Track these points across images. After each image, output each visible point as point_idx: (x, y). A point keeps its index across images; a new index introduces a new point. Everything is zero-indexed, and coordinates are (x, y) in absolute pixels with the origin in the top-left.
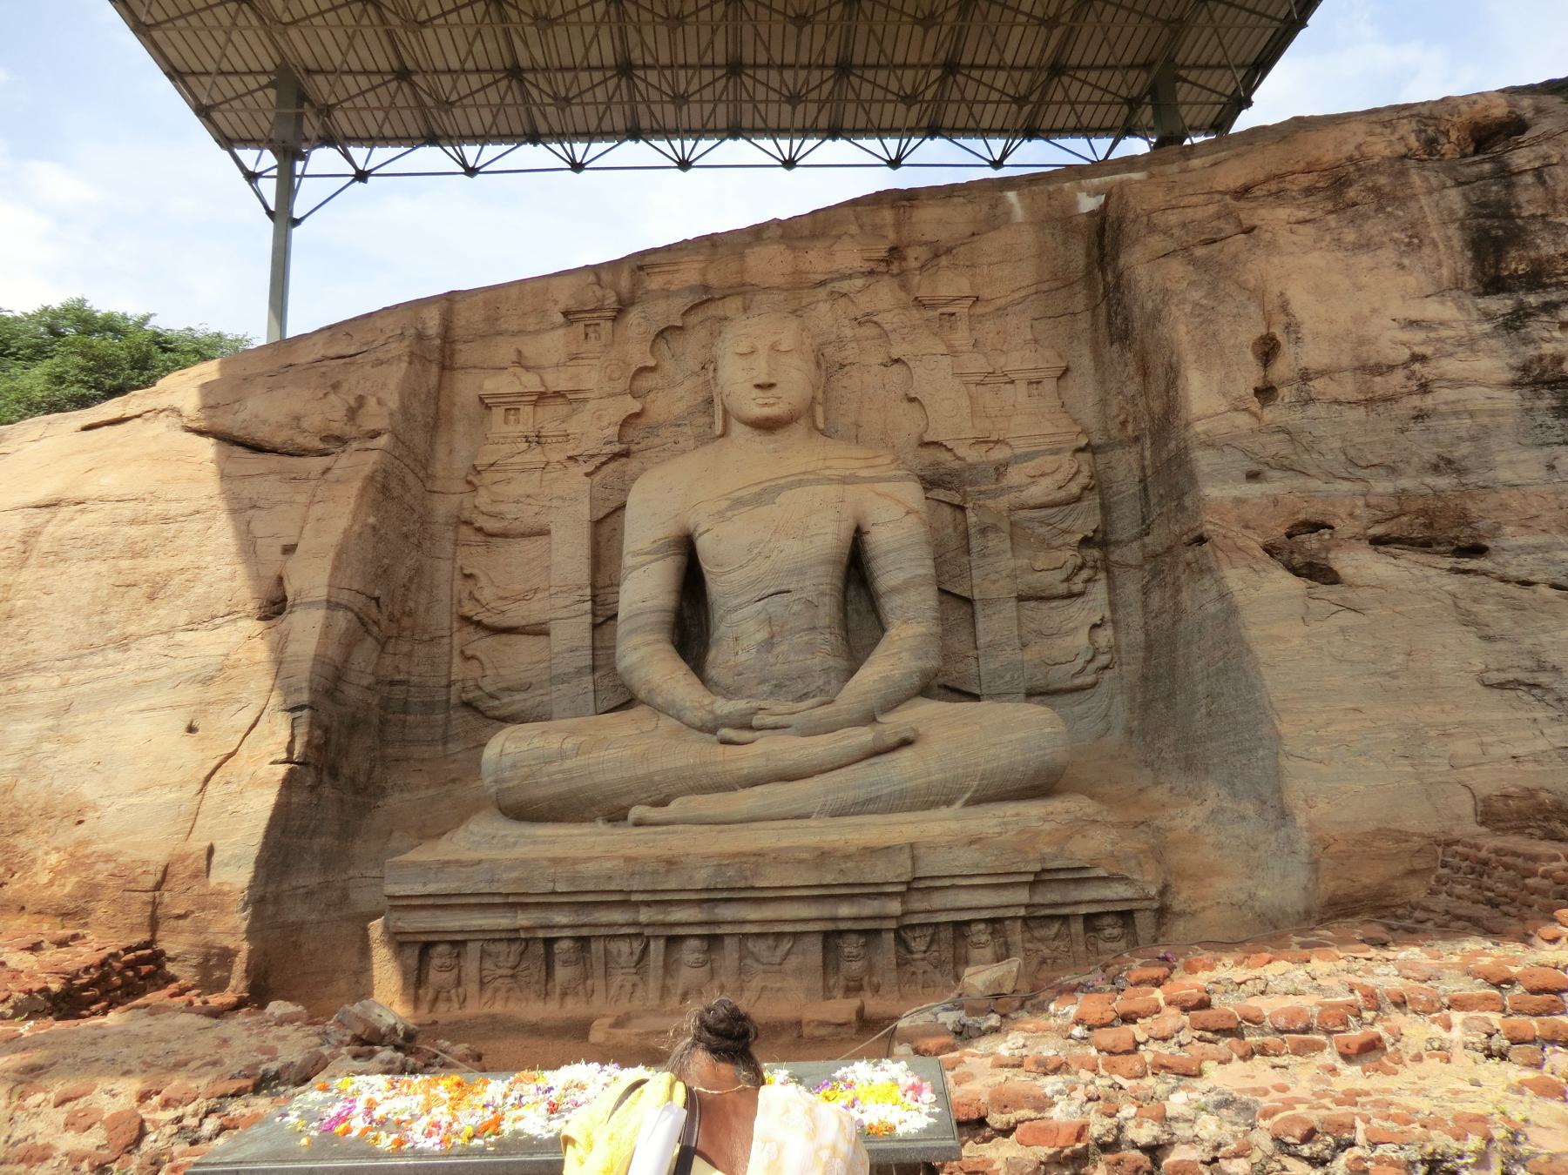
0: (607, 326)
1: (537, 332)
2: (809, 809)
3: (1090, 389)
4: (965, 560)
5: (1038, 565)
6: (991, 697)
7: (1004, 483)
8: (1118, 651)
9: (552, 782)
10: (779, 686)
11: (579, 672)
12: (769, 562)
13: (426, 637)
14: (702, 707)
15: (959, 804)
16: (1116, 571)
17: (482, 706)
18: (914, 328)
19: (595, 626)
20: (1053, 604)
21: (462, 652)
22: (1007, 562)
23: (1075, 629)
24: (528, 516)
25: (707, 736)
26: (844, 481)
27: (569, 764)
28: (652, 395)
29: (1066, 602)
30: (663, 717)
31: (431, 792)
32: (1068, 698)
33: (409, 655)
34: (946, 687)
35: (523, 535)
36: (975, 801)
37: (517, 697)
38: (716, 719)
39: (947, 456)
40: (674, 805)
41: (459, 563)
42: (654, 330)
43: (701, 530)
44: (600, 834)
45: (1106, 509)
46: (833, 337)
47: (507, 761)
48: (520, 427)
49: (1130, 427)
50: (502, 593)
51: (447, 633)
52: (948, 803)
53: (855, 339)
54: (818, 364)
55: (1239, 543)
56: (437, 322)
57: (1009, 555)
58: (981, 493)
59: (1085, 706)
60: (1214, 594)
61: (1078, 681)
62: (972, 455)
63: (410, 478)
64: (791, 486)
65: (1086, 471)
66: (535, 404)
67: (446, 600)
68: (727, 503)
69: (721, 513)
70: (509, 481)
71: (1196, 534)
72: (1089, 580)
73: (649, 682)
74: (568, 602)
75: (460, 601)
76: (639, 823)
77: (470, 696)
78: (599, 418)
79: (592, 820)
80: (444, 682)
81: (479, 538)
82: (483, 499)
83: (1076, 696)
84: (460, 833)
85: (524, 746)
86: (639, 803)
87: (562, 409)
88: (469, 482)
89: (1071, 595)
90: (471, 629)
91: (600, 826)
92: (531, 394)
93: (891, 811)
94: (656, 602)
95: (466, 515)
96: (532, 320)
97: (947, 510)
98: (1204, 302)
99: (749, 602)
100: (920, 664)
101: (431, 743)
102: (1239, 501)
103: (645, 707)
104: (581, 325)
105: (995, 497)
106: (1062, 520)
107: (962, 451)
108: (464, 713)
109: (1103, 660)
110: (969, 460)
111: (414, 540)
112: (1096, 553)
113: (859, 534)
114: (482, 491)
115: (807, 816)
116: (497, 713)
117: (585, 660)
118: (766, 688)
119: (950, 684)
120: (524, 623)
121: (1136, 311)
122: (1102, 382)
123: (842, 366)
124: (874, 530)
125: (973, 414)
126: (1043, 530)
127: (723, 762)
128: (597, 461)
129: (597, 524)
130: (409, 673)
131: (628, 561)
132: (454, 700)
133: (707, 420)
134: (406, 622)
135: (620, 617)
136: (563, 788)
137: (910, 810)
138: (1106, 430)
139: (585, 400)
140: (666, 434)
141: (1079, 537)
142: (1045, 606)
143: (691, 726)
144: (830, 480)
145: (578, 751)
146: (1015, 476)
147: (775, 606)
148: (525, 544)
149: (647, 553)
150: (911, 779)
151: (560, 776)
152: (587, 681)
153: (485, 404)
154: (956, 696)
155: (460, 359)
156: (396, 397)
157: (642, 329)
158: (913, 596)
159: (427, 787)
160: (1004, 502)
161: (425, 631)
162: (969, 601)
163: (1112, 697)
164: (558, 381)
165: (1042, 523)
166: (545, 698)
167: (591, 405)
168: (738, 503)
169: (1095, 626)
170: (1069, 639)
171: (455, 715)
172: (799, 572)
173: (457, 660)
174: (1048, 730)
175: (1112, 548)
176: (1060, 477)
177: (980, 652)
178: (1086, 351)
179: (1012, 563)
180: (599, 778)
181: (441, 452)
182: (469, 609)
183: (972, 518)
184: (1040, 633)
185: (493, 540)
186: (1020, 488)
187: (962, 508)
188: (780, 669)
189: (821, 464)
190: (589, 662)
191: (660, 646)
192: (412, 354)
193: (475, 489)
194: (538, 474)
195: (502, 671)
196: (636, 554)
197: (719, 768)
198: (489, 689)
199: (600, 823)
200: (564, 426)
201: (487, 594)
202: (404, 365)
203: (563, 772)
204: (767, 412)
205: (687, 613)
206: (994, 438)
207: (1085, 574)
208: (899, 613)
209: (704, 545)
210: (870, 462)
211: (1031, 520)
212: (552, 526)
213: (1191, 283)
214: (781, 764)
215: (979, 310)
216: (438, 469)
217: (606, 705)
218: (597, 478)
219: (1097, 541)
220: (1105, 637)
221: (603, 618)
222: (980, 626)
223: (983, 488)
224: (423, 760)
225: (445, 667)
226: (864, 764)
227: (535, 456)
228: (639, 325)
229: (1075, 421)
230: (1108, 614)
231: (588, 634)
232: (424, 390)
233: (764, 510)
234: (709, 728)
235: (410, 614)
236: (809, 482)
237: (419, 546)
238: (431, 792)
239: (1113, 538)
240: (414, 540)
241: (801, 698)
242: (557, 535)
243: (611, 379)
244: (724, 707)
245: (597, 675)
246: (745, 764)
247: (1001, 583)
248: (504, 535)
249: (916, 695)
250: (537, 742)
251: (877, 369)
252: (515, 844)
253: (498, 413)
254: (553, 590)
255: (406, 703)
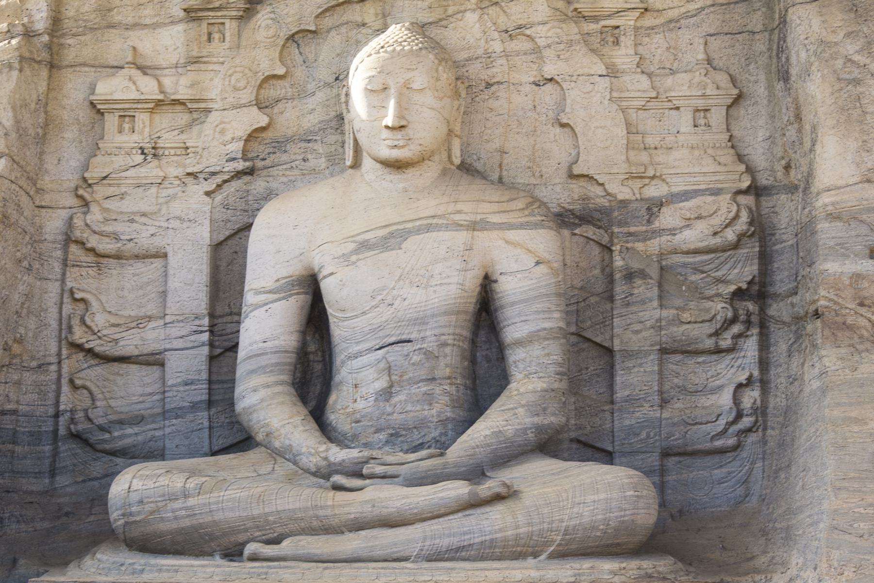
0: (230, 27)
1: (155, 26)
2: (407, 554)
3: (762, 122)
4: (608, 306)
5: (686, 316)
6: (623, 454)
7: (656, 224)
8: (764, 414)
9: (176, 518)
10: (396, 435)
11: (194, 407)
12: (392, 310)
13: (34, 364)
14: (317, 453)
15: (542, 557)
16: (773, 327)
17: (93, 439)
18: (570, 43)
19: (212, 358)
20: (700, 359)
21: (71, 381)
22: (652, 313)
23: (721, 388)
24: (144, 236)
25: (322, 481)
26: (474, 227)
27: (191, 502)
28: (280, 105)
29: (715, 357)
30: (280, 460)
31: (46, 524)
32: (708, 460)
33: (18, 383)
34: (579, 441)
35: (137, 257)
36: (563, 554)
37: (129, 431)
38: (330, 465)
39: (599, 191)
40: (285, 543)
41: (69, 284)
42: (284, 33)
43: (325, 272)
44: (218, 566)
45: (765, 258)
46: (480, 52)
47: (135, 497)
48: (135, 137)
49: (793, 172)
50: (113, 320)
51: (53, 359)
52: (535, 555)
53: (506, 55)
54: (457, 94)
55: (849, 321)
56: (44, 14)
57: (655, 303)
58: (630, 234)
59: (724, 470)
60: (817, 371)
61: (718, 443)
62: (623, 193)
63: (25, 200)
64: (418, 231)
65: (744, 217)
66: (152, 111)
67: (54, 324)
68: (352, 246)
69: (345, 257)
70: (122, 196)
71: (812, 308)
72: (740, 336)
73: (268, 425)
74: (184, 332)
75: (70, 328)
76: (254, 558)
77: (80, 427)
78: (222, 132)
79: (211, 554)
80: (51, 411)
81: (91, 258)
82: (95, 216)
83: (717, 458)
84: (88, 561)
85: (150, 484)
86: (254, 540)
87: (183, 118)
88: (78, 196)
89: (718, 351)
90: (81, 355)
91: (218, 560)
92: (146, 101)
93: (482, 559)
94: (277, 342)
95: (77, 234)
96: (148, 11)
97: (596, 250)
98: (856, 58)
99: (369, 350)
100: (536, 420)
101: (38, 474)
102: (857, 277)
103: (263, 449)
104: (204, 25)
105: (645, 240)
106: (717, 269)
107: (612, 188)
108: (73, 445)
109: (747, 422)
110: (620, 197)
111: (25, 263)
112: (751, 306)
113: (487, 283)
114: (94, 208)
115: (406, 559)
116: (107, 447)
117: (200, 393)
118: (382, 436)
119: (582, 439)
120: (137, 353)
121: (793, 60)
122: (773, 117)
123: (489, 85)
124: (502, 279)
125: (629, 146)
126: (695, 278)
127: (333, 506)
128: (219, 179)
129: (217, 247)
130: (18, 402)
131: (249, 298)
132: (62, 431)
133: (339, 137)
134: (16, 349)
135: (242, 353)
136: (186, 523)
137: (500, 559)
138: (773, 170)
139: (208, 111)
140: (295, 150)
141: (733, 288)
142: (691, 361)
143: (307, 471)
144: (458, 226)
145: (200, 490)
146: (668, 218)
147: (395, 355)
148: (139, 267)
149: (270, 292)
150: (500, 530)
151: (184, 513)
152: (202, 417)
153: (97, 110)
154: (589, 452)
155: (70, 56)
156: (11, 114)
157: (271, 32)
158: (536, 350)
159: (42, 519)
160: (654, 246)
161: (33, 358)
162: (610, 351)
163: (753, 463)
164: (180, 86)
165: (697, 270)
166: (158, 433)
167: (214, 117)
168: (364, 246)
169: (740, 386)
170: (714, 397)
171: (63, 447)
172: (421, 321)
173: (65, 388)
174: (631, 493)
175: (770, 301)
176: (717, 221)
177: (616, 407)
178: (762, 77)
179: (657, 314)
180: (219, 516)
181: (50, 162)
182: (79, 335)
183: (618, 262)
184: (683, 389)
185: (105, 261)
186: (673, 232)
187: (608, 249)
188: (397, 418)
189: (451, 208)
190: (205, 397)
191: (280, 388)
192: (22, 58)
193: (86, 204)
194: (154, 190)
195: (112, 403)
196: (258, 292)
197: (329, 512)
198: (101, 421)
199: (218, 557)
200: (183, 137)
201: (99, 320)
202: (15, 74)
203: (186, 508)
204: (395, 154)
205: (312, 348)
206: (651, 173)
207: (736, 329)
208: (521, 366)
209: (327, 287)
210: (505, 207)
211: (684, 265)
212: (169, 249)
213: (848, 35)
214: (385, 511)
215: (648, 21)
216: (46, 182)
217: (218, 444)
218: (219, 198)
219: (758, 292)
220: (751, 397)
221: (223, 348)
222: (618, 379)
223: (632, 229)
224: (32, 492)
225: (51, 395)
226: (460, 514)
227: (151, 171)
228: (268, 27)
229: (740, 158)
230: (756, 373)
231: (204, 367)
232: (35, 97)
233: (389, 256)
234: (324, 474)
235: (20, 341)
236: (437, 228)
237: (29, 269)
238: (46, 524)
239: (771, 290)
240: (25, 263)
241: (415, 449)
242: (173, 260)
243: (236, 89)
244: (337, 454)
245: (213, 410)
246: (353, 510)
247: (644, 334)
248: (118, 257)
249: (532, 451)
250: (163, 481)
251: (528, 88)
252: (142, 571)
253: (111, 121)
254: (168, 319)
255: (15, 432)
